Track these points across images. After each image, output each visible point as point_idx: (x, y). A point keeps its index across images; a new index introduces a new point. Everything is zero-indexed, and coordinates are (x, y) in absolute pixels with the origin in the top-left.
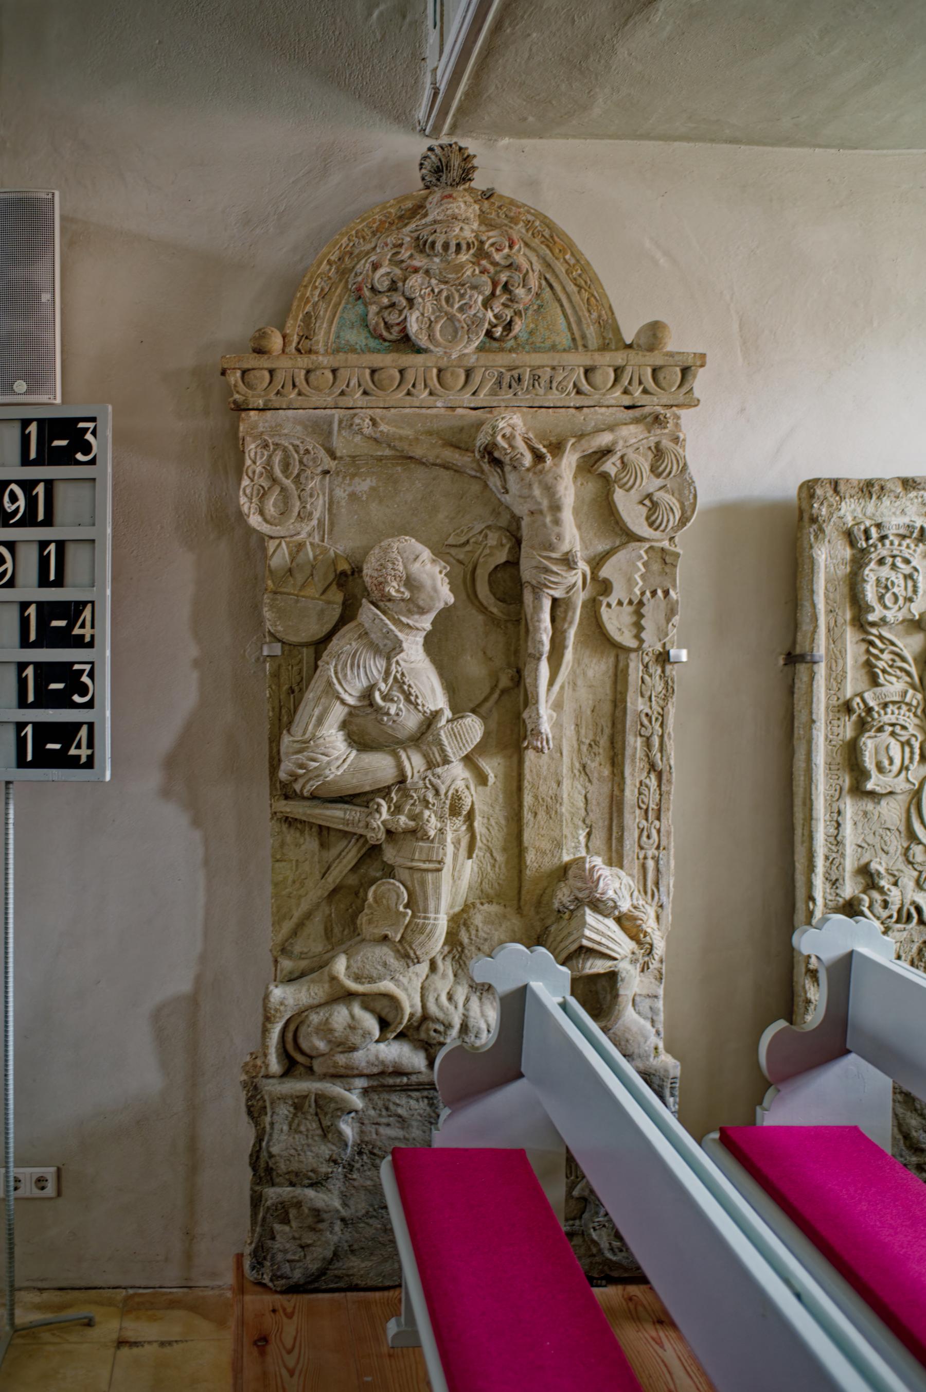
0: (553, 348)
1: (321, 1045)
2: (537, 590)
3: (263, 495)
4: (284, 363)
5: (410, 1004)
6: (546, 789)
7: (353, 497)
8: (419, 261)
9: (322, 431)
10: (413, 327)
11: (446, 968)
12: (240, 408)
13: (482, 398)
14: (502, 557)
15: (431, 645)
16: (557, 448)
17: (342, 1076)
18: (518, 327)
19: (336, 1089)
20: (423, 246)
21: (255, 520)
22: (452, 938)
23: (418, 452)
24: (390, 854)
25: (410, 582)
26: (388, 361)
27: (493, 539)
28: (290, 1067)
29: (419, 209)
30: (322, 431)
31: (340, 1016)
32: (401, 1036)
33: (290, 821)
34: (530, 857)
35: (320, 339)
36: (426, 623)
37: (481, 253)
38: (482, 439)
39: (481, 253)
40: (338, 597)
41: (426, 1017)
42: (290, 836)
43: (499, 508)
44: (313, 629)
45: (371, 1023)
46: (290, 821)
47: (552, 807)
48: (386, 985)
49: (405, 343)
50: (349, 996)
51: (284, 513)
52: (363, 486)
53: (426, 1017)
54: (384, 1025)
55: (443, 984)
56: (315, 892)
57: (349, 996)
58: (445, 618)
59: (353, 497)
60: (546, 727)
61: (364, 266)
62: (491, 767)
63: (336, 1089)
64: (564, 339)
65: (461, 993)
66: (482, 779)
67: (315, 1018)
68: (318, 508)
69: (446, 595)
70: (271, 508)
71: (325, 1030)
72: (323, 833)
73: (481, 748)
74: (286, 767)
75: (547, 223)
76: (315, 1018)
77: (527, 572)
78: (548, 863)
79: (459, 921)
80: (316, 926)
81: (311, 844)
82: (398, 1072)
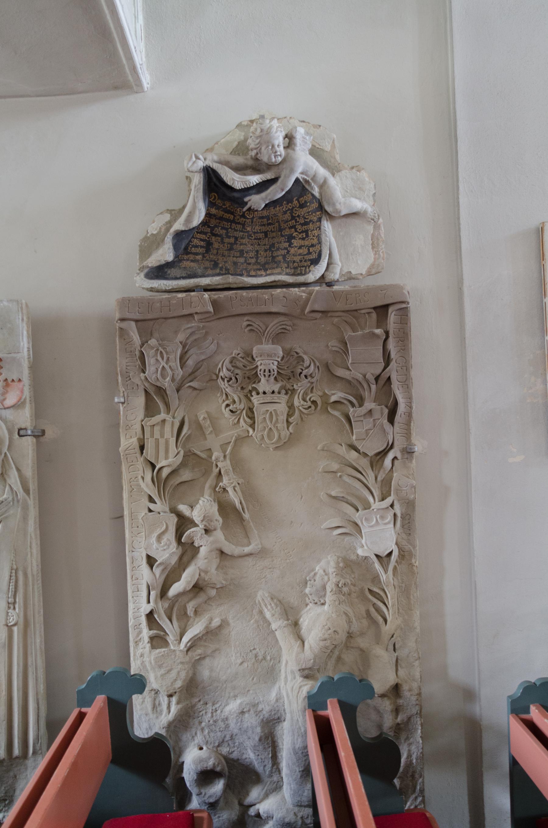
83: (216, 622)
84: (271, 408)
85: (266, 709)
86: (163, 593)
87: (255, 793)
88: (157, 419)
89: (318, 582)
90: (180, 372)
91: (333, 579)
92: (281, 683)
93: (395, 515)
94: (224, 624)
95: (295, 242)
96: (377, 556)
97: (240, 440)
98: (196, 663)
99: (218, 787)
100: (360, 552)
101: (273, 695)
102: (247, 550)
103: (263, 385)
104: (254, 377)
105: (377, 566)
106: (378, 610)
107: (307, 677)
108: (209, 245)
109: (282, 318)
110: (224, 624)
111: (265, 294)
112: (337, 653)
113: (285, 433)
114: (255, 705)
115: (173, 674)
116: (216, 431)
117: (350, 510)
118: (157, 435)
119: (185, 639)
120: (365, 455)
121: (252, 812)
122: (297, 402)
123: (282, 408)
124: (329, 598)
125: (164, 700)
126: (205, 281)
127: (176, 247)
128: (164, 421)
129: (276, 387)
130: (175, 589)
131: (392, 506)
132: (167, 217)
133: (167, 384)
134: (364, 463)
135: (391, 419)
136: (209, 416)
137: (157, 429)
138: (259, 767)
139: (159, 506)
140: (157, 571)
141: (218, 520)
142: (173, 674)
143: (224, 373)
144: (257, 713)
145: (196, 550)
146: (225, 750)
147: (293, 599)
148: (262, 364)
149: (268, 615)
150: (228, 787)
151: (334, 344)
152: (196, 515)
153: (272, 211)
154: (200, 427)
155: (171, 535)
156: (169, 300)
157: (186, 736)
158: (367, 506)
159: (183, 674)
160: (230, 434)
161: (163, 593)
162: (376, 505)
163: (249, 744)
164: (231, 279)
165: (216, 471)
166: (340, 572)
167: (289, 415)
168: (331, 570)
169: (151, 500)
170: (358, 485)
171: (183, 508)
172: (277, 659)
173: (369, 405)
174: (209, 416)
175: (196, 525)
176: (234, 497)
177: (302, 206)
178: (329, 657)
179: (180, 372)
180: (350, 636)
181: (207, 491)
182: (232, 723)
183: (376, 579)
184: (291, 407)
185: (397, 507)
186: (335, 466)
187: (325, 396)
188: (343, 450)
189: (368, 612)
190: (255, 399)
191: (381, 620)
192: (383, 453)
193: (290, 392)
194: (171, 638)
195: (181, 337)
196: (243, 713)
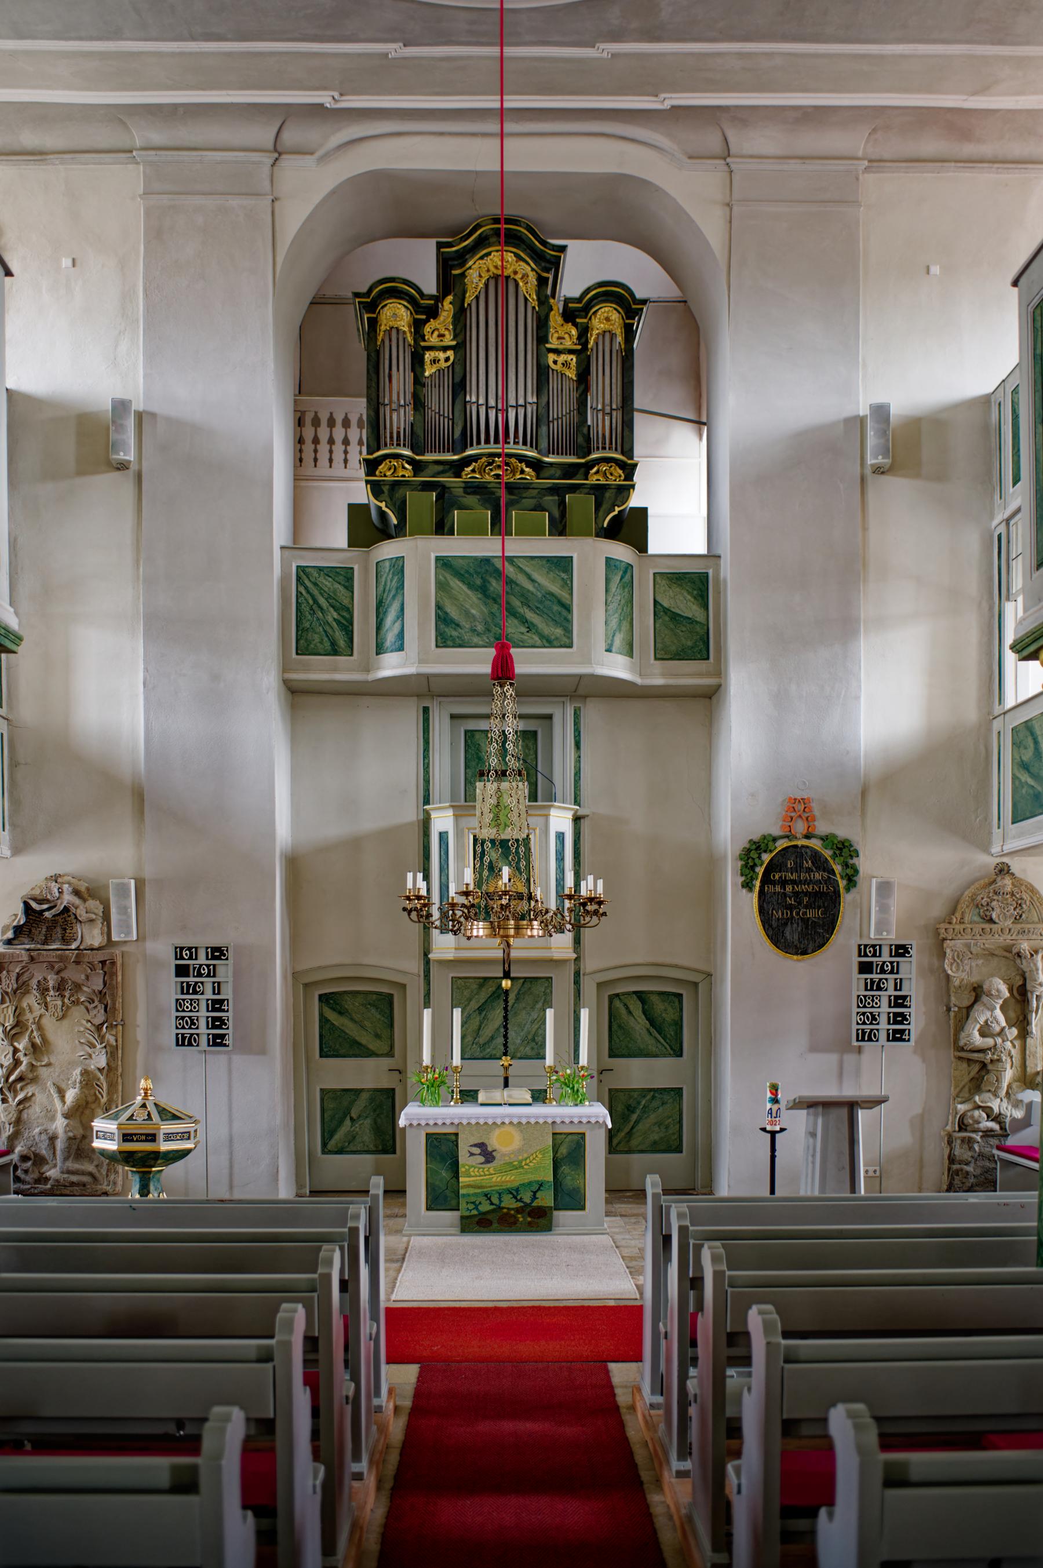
0: (1033, 922)
1: (971, 1121)
2: (1032, 993)
3: (952, 964)
4: (957, 927)
5: (996, 1110)
6: (1033, 1049)
7: (977, 965)
8: (995, 897)
9: (968, 946)
10: (994, 916)
11: (1005, 1100)
12: (944, 939)
13: (1014, 937)
14: (1021, 983)
15: (1002, 1008)
16: (1036, 952)
17: (975, 1131)
18: (1024, 916)
19: (974, 1135)
20: (995, 893)
21: (949, 972)
22: (1007, 1093)
23: (996, 953)
24: (990, 1067)
25: (998, 991)
26: (987, 926)
27: (1018, 978)
28: (961, 1129)
29: (994, 881)
30: (968, 946)
31: (976, 1113)
32: (992, 1120)
33: (960, 1058)
34: (1028, 1069)
35: (966, 919)
36: (1001, 1002)
37: (1013, 895)
38: (1015, 951)
39: (1013, 895)
40: (974, 994)
41: (1000, 1114)
42: (959, 1063)
43: (1019, 969)
44: (966, 1003)
45: (984, 1115)
46: (960, 1058)
47: (1034, 1055)
48: (989, 1104)
49: (991, 921)
50: (979, 1107)
51: (958, 970)
52: (980, 962)
53: (1000, 1114)
54: (988, 1117)
55: (1005, 1104)
56: (966, 1079)
57: (979, 1107)
58: (1005, 1001)
59: (977, 965)
60: (1034, 1031)
61: (979, 898)
62: (1017, 1043)
63: (974, 1135)
64: (1036, 919)
65: (1010, 1108)
66: (1014, 1046)
67: (969, 1114)
68: (967, 968)
69: (1007, 995)
70: (954, 969)
71: (972, 1117)
72: (969, 1061)
73: (1015, 1038)
74: (962, 1043)
75: (1032, 886)
76: (969, 1114)
77: (1028, 987)
78: (1033, 1071)
79: (1009, 1086)
80: (966, 1089)
81: (965, 1065)
82: (992, 1130)
83: (30, 1094)
84: (55, 1003)
85: (51, 1132)
86: (7, 1080)
87: (45, 1168)
88: (5, 1006)
89: (73, 1079)
90: (15, 986)
91: (79, 1077)
92: (57, 1122)
93: (107, 1052)
94: (33, 1095)
95: (68, 931)
96: (99, 1069)
97: (41, 1016)
98: (20, 1112)
99: (29, 1164)
100: (92, 1067)
101: (54, 1127)
102: (43, 1063)
103: (52, 993)
104: (47, 990)
105: (99, 1074)
106: (100, 1092)
107: (66, 1118)
108: (30, 931)
109: (61, 964)
110: (33, 1095)
111: (54, 953)
112: (81, 1110)
113: (61, 1014)
114: (46, 1130)
115: (11, 1115)
116: (31, 1011)
117: (88, 1049)
118: (5, 1012)
119: (16, 1100)
120: (94, 1025)
121: (44, 1176)
122: (66, 1000)
123: (59, 1003)
124: (78, 1085)
125: (7, 1126)
126: (27, 947)
127: (15, 932)
128: (8, 1007)
129: (57, 994)
130: (12, 1078)
131: (105, 1047)
132: (14, 917)
133: (9, 990)
134: (93, 1029)
135: (106, 1010)
136: (29, 1005)
137: (5, 1010)
138: (48, 1158)
139: (5, 1043)
140: (5, 1070)
141: (32, 1050)
142: (11, 1115)
143: (35, 987)
144: (47, 1134)
145: (22, 1063)
146: (33, 1149)
147: (63, 1086)
148: (51, 984)
149: (52, 1092)
150: (34, 1164)
151: (83, 977)
152: (20, 1047)
153: (57, 918)
154: (24, 1010)
155: (10, 1055)
156: (12, 954)
157: (16, 1142)
158: (95, 1047)
159: (15, 1116)
160: (37, 1014)
161: (7, 1080)
162: (99, 1046)
163: (43, 1147)
164: (39, 946)
165: (30, 1029)
166: (82, 1074)
167: (63, 1006)
168: (78, 1073)
169: (3, 1040)
170: (91, 1038)
171: (16, 1044)
172: (56, 1111)
173: (96, 1003)
174: (29, 1005)
175: (20, 1051)
176: (38, 1041)
177: (69, 916)
178: (77, 1110)
179: (15, 986)
180: (87, 1103)
181: (27, 1038)
182: (36, 1137)
183: (99, 1079)
184: (63, 1003)
185: (108, 1047)
186: (82, 1029)
187: (78, 999)
188: (84, 1022)
189: (95, 1093)
190: (48, 999)
191: (100, 1096)
192: (102, 1024)
193: (63, 996)
194: (10, 1100)
195: (17, 970)
196: (41, 1133)
